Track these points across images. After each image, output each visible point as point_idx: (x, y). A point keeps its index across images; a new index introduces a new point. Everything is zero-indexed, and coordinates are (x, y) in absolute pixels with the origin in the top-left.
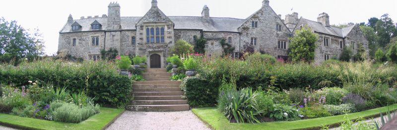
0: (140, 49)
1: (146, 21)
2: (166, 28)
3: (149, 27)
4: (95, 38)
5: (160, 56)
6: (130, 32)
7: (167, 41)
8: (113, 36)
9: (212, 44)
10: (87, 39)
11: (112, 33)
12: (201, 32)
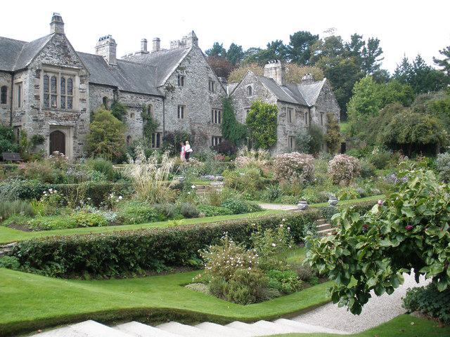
0: (36, 120)
1: (47, 62)
2: (77, 80)
5: (63, 136)
7: (77, 106)
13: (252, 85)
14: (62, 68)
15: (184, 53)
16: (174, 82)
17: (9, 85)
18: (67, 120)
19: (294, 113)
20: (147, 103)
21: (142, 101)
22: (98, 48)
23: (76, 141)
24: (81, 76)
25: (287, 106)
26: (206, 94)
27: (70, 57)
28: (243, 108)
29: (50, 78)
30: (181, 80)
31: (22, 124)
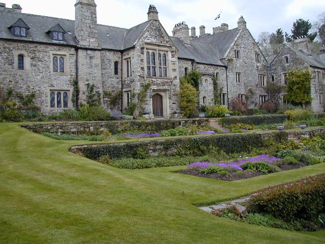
2: (170, 54)
3: (149, 51)
4: (59, 57)
5: (161, 97)
6: (112, 53)
7: (171, 74)
9: (206, 80)
10: (46, 59)
11: (89, 52)
12: (192, 63)
13: (288, 55)
14: (159, 46)
15: (237, 33)
16: (232, 55)
17: (119, 60)
20: (216, 72)
21: (211, 70)
22: (174, 32)
24: (172, 52)
25: (316, 70)
26: (254, 64)
28: (282, 73)
29: (150, 54)
30: (237, 53)
31: (132, 89)
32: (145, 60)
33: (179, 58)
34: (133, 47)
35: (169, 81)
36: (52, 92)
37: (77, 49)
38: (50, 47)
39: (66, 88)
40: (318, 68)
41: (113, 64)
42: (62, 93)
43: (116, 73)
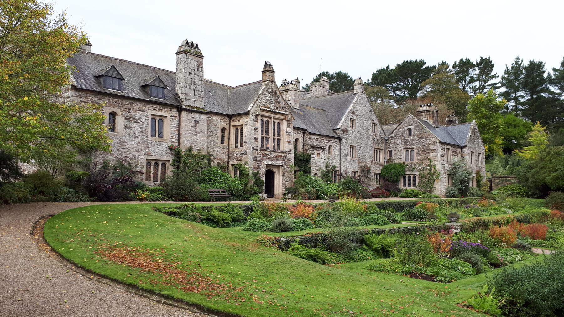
0: (255, 160)
2: (285, 122)
4: (158, 118)
8: (196, 122)
9: (318, 154)
10: (143, 120)
12: (303, 133)
13: (412, 127)
17: (227, 127)
18: (278, 160)
19: (450, 152)
20: (328, 144)
23: (284, 178)
25: (445, 146)
27: (279, 103)
29: (264, 122)
32: (259, 130)
33: (294, 128)
34: (247, 114)
35: (283, 155)
36: (149, 162)
37: (180, 110)
38: (149, 106)
39: (165, 158)
40: (448, 144)
41: (219, 131)
42: (160, 163)
43: (222, 141)
